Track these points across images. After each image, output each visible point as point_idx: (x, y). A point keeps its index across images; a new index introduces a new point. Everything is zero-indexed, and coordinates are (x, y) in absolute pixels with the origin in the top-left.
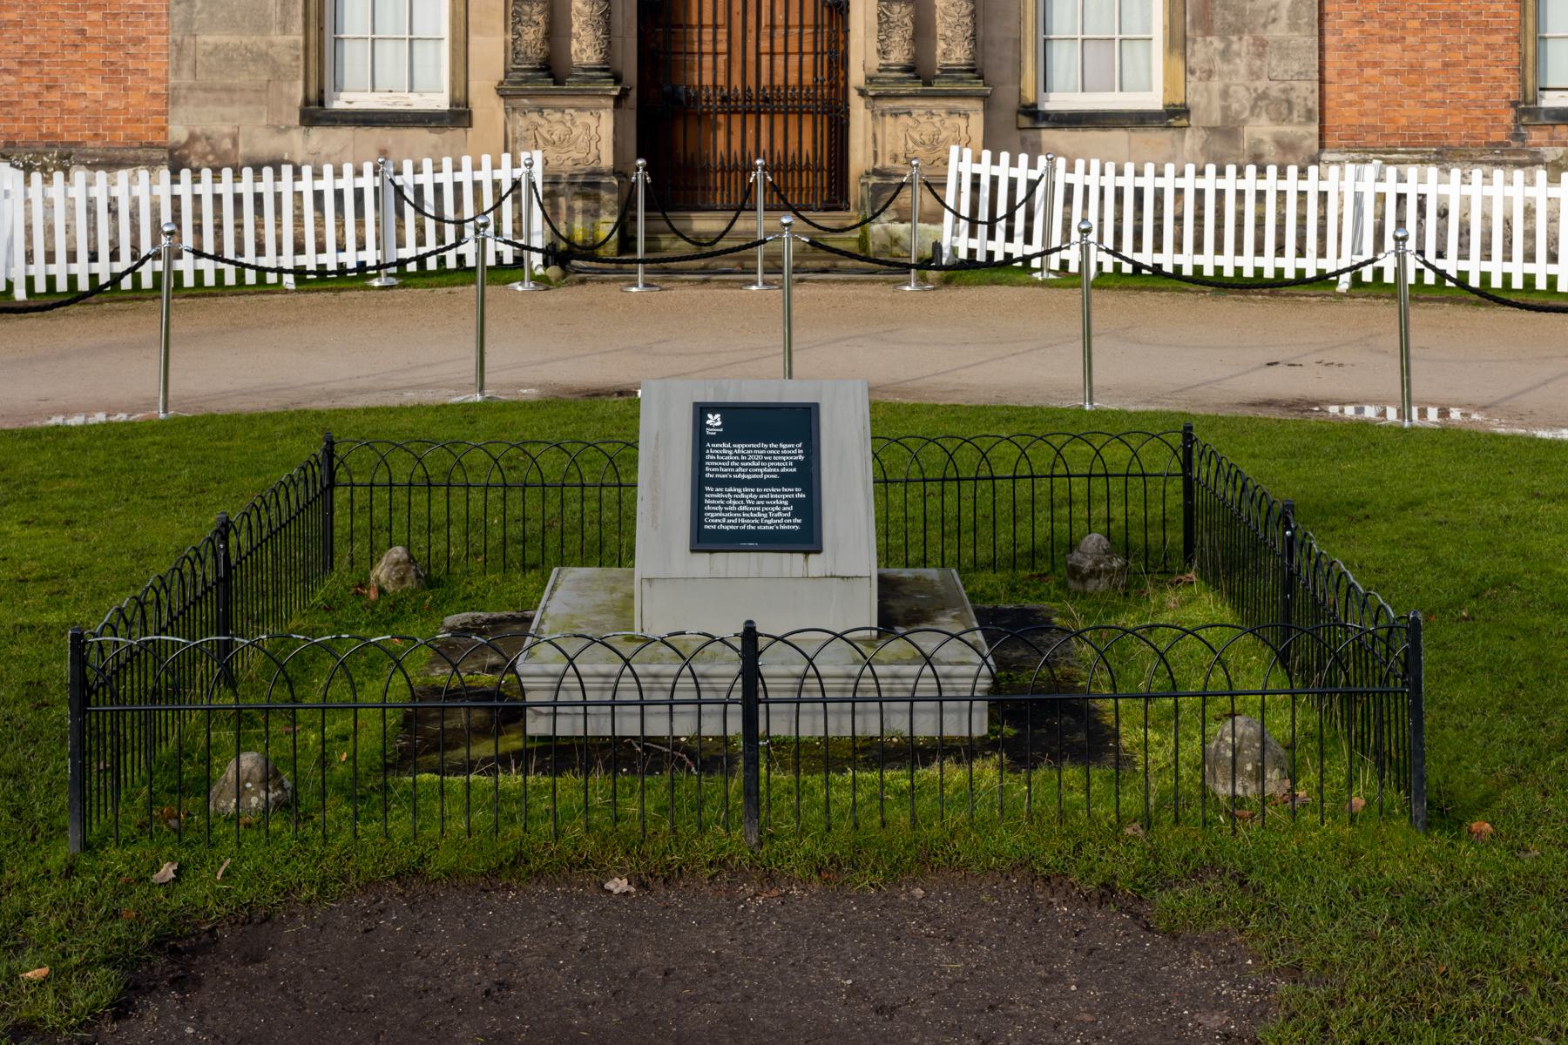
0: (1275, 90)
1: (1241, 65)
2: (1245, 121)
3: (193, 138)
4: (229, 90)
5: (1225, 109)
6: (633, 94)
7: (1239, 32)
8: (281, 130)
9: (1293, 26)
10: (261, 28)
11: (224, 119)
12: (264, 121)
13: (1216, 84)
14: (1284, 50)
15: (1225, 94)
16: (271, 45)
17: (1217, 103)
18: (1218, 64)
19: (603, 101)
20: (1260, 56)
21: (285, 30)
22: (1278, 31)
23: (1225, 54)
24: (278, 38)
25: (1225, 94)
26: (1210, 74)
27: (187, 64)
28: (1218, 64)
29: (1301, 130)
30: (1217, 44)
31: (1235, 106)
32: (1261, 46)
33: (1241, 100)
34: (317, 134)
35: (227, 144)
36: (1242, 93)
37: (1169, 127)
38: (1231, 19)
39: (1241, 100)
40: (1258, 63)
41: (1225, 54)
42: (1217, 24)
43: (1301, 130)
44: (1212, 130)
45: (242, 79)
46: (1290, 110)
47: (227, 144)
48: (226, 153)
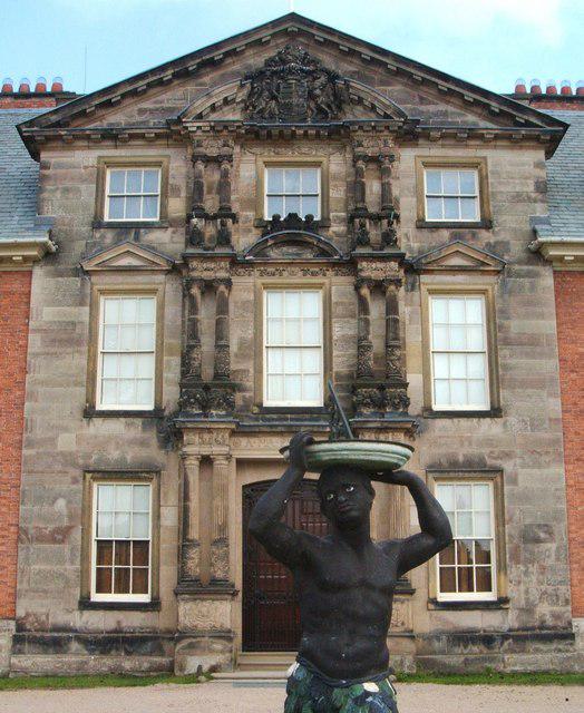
0: (550, 589)
1: (534, 578)
2: (535, 606)
3: (28, 615)
4: (45, 592)
5: (527, 599)
6: (240, 595)
7: (532, 562)
8: (69, 611)
9: (558, 559)
10: (61, 561)
11: (42, 606)
12: (62, 606)
13: (522, 587)
14: (553, 570)
15: (527, 592)
16: (66, 570)
17: (523, 596)
18: (523, 578)
19: (226, 596)
20: (542, 573)
21: (72, 563)
22: (550, 562)
23: (526, 573)
24: (68, 566)
25: (527, 592)
26: (519, 582)
27: (25, 579)
28: (523, 578)
29: (563, 609)
30: (522, 568)
31: (532, 598)
32: (543, 570)
33: (534, 595)
34: (87, 614)
35: (44, 618)
36: (535, 591)
37: (501, 608)
38: (528, 556)
39: (534, 595)
40: (541, 577)
41: (526, 573)
42: (522, 558)
43: (563, 609)
44: (521, 610)
45: (52, 586)
46: (558, 600)
47: (44, 618)
48: (43, 622)
